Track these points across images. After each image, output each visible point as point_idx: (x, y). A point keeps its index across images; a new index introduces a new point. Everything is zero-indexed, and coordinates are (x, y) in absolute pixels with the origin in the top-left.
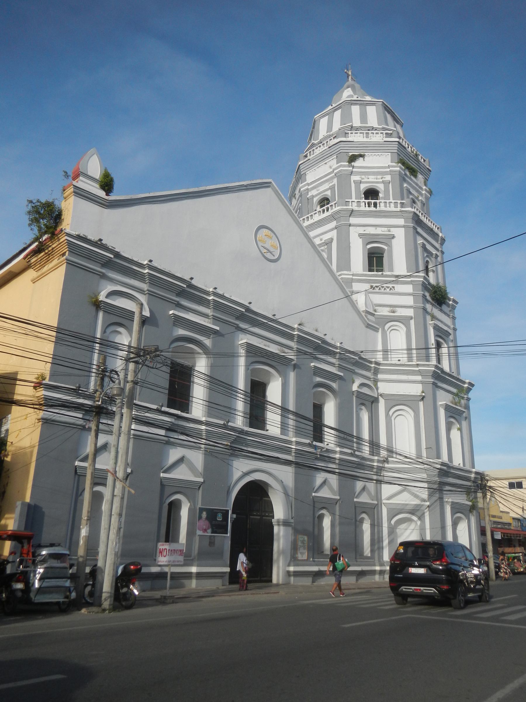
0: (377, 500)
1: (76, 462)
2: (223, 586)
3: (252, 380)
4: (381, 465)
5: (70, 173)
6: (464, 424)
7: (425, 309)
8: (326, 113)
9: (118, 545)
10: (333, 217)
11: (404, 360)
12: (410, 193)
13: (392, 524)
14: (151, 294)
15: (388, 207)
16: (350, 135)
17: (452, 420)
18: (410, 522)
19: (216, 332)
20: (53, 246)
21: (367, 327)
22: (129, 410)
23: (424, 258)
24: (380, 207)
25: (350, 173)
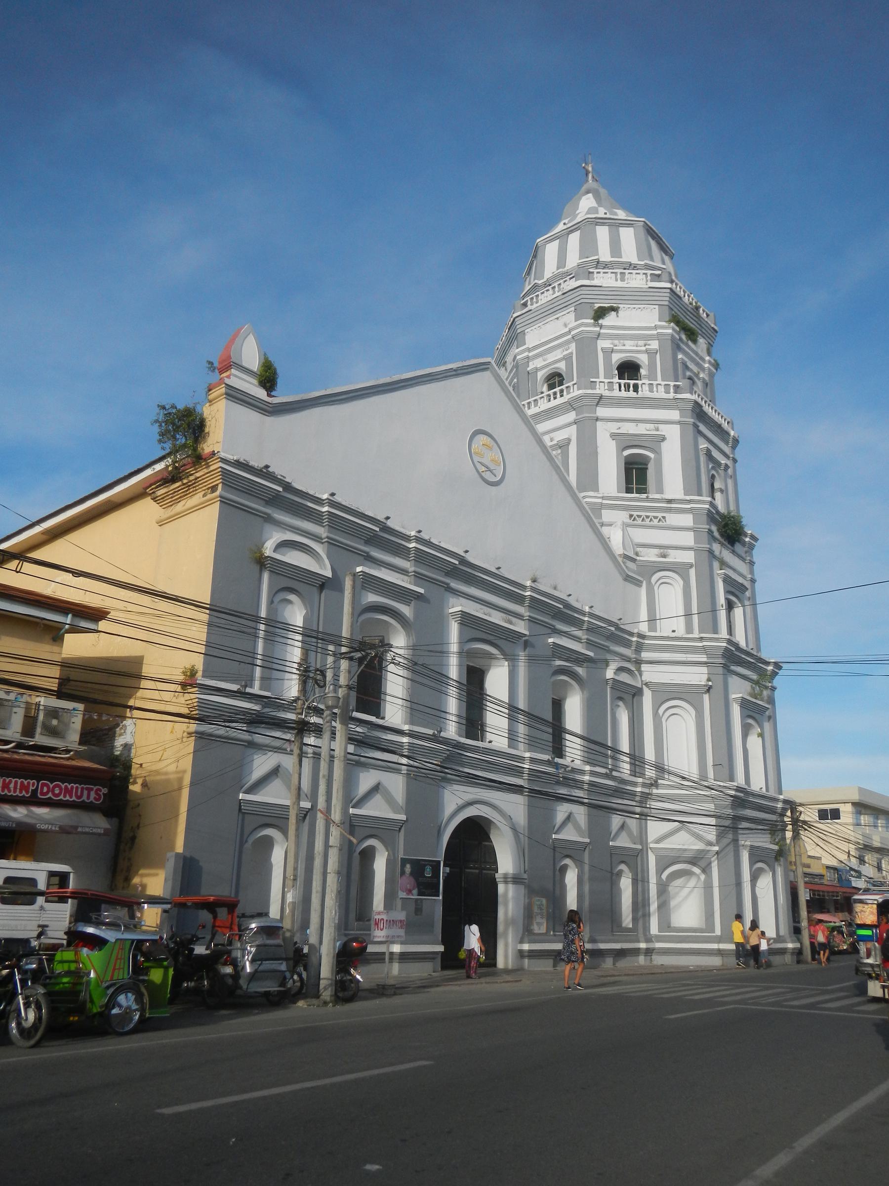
0: (641, 844)
1: (241, 794)
2: (434, 972)
3: (468, 666)
4: (646, 790)
5: (216, 364)
6: (767, 726)
7: (711, 552)
8: (555, 236)
9: (338, 914)
10: (570, 406)
11: (681, 632)
12: (687, 368)
13: (663, 880)
14: (332, 543)
15: (655, 392)
16: (595, 275)
17: (750, 721)
18: (688, 877)
19: (419, 597)
20: (198, 475)
21: (625, 580)
22: (344, 727)
23: (709, 471)
24: (642, 391)
25: (596, 336)
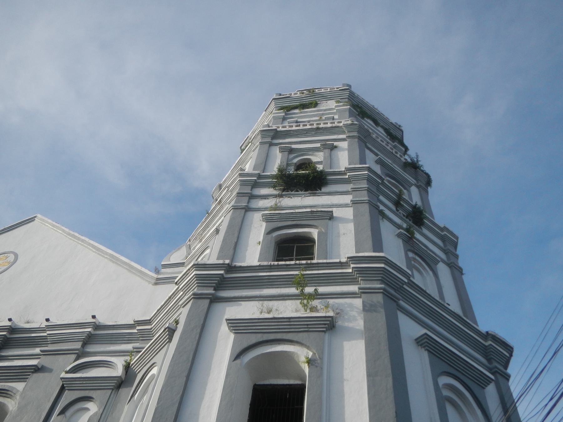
21: (156, 284)
